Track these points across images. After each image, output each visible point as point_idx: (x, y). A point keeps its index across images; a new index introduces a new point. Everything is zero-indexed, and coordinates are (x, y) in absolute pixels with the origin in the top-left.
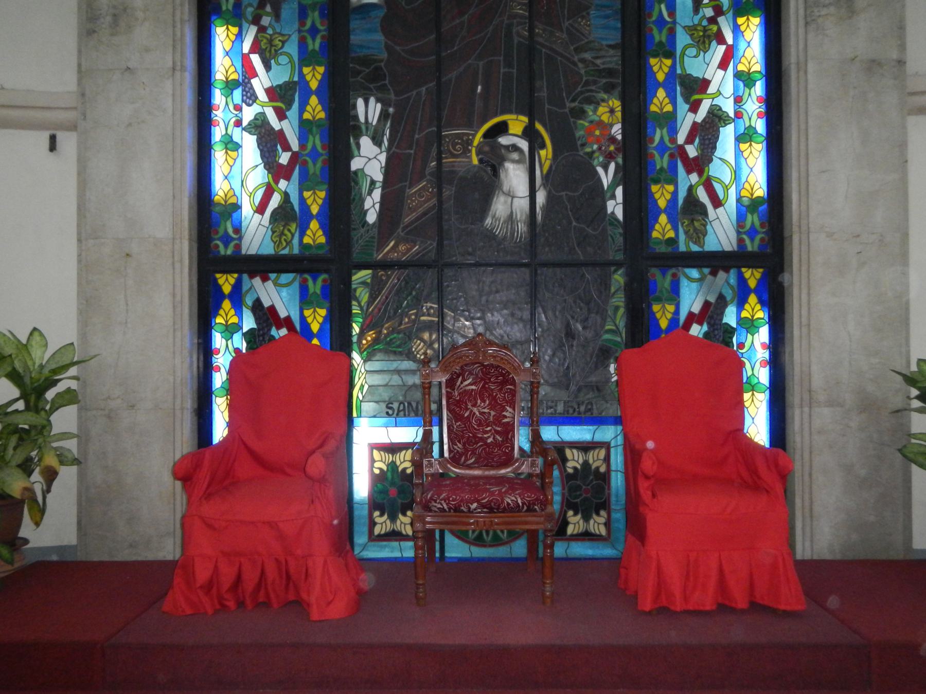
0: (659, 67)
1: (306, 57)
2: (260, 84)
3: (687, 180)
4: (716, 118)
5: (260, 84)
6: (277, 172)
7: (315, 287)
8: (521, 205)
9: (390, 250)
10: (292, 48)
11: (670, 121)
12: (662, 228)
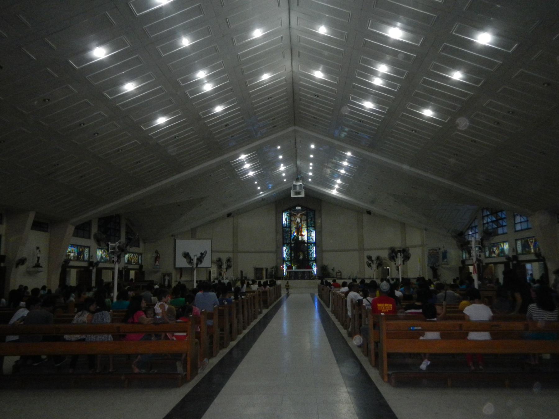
0: (309, 250)
1: (289, 249)
2: (286, 251)
4: (312, 253)
5: (286, 251)
6: (287, 256)
8: (301, 258)
11: (310, 253)
12: (309, 259)
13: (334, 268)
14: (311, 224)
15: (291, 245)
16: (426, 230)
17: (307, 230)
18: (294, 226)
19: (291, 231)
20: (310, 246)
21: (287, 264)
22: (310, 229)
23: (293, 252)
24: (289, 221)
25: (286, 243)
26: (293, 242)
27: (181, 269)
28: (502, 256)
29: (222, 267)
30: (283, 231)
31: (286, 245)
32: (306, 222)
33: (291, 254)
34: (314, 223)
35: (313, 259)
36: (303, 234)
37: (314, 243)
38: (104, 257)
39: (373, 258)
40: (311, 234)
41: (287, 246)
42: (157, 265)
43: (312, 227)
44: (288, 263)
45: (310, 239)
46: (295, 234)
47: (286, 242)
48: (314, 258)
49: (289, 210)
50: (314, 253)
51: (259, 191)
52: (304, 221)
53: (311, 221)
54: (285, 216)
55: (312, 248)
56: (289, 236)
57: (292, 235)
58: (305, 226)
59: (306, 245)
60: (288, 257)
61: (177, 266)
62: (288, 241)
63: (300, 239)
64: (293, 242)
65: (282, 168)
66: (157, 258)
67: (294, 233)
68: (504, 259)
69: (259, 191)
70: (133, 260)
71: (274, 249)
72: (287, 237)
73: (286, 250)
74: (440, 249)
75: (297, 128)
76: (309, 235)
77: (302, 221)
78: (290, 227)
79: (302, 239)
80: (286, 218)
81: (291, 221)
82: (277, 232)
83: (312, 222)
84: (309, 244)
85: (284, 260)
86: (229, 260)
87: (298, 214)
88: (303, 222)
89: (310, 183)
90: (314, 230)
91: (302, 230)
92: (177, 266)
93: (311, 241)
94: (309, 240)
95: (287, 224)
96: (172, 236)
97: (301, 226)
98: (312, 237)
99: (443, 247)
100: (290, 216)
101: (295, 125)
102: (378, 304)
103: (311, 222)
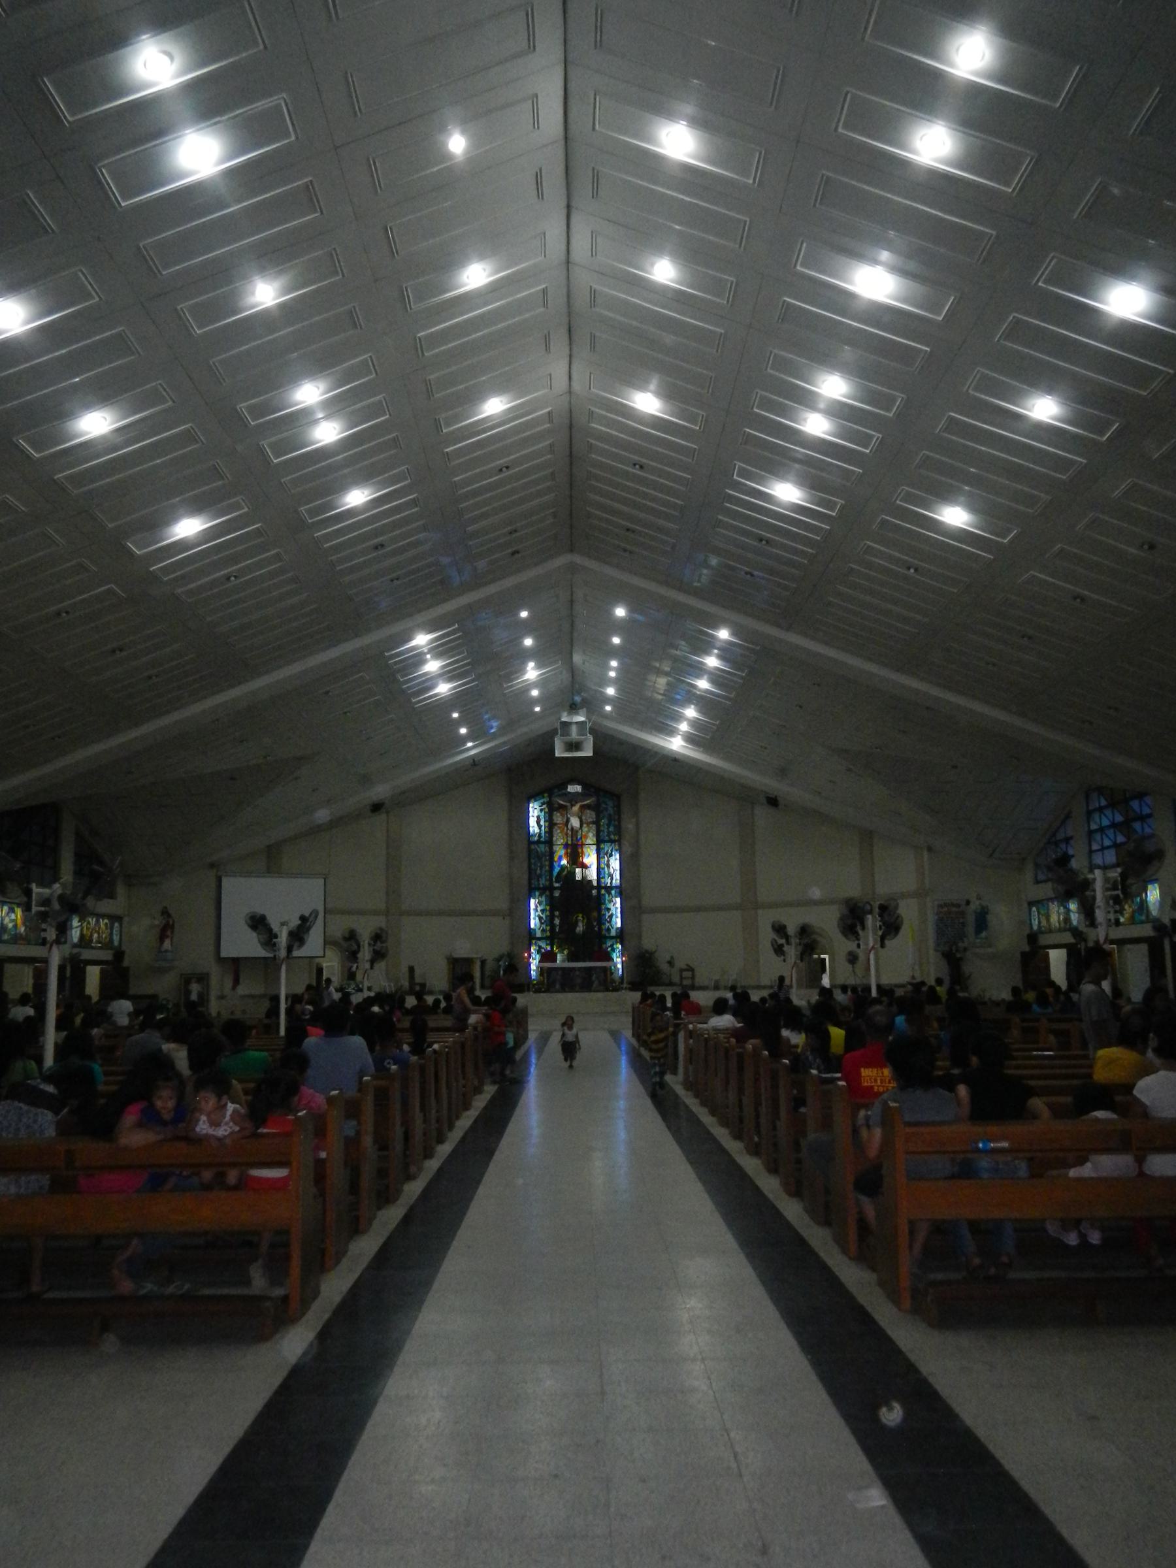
0: (603, 907)
1: (546, 905)
2: (539, 909)
3: (608, 924)
4: (612, 915)
5: (539, 909)
7: (548, 942)
8: (582, 929)
9: (560, 936)
10: (544, 903)
11: (605, 915)
12: (604, 932)
13: (672, 957)
14: (609, 835)
15: (551, 894)
16: (930, 849)
17: (598, 852)
18: (559, 840)
19: (551, 854)
20: (607, 895)
21: (540, 947)
22: (607, 847)
23: (557, 913)
24: (547, 824)
25: (539, 889)
26: (556, 885)
27: (236, 961)
28: (1142, 922)
29: (360, 955)
30: (530, 851)
31: (537, 894)
32: (594, 827)
33: (551, 918)
34: (619, 830)
35: (613, 933)
36: (586, 861)
37: (616, 887)
38: (10, 925)
39: (791, 930)
40: (608, 861)
41: (541, 895)
42: (166, 951)
43: (612, 841)
44: (542, 944)
45: (606, 876)
46: (564, 862)
47: (539, 884)
48: (617, 928)
49: (546, 795)
50: (617, 917)
51: (465, 740)
52: (588, 824)
53: (609, 825)
54: (535, 811)
55: (611, 901)
56: (547, 868)
57: (556, 865)
58: (591, 839)
59: (594, 892)
60: (544, 926)
61: (223, 954)
62: (543, 882)
63: (578, 877)
64: (556, 885)
65: (531, 673)
66: (166, 931)
67: (560, 858)
68: (1147, 931)
69: (465, 740)
70: (96, 935)
71: (502, 904)
72: (541, 869)
73: (536, 907)
74: (968, 903)
75: (578, 559)
76: (602, 866)
77: (585, 825)
78: (550, 842)
79: (584, 878)
80: (538, 817)
81: (551, 825)
82: (512, 857)
83: (611, 829)
84: (603, 892)
85: (531, 936)
86: (377, 937)
87: (575, 805)
88: (585, 829)
89: (606, 716)
90: (616, 850)
91: (584, 850)
92: (223, 954)
93: (609, 881)
94: (603, 880)
95: (540, 834)
96: (212, 866)
97: (581, 838)
98: (612, 871)
99: (979, 898)
100: (551, 810)
101: (572, 551)
102: (862, 1070)
103: (608, 829)
